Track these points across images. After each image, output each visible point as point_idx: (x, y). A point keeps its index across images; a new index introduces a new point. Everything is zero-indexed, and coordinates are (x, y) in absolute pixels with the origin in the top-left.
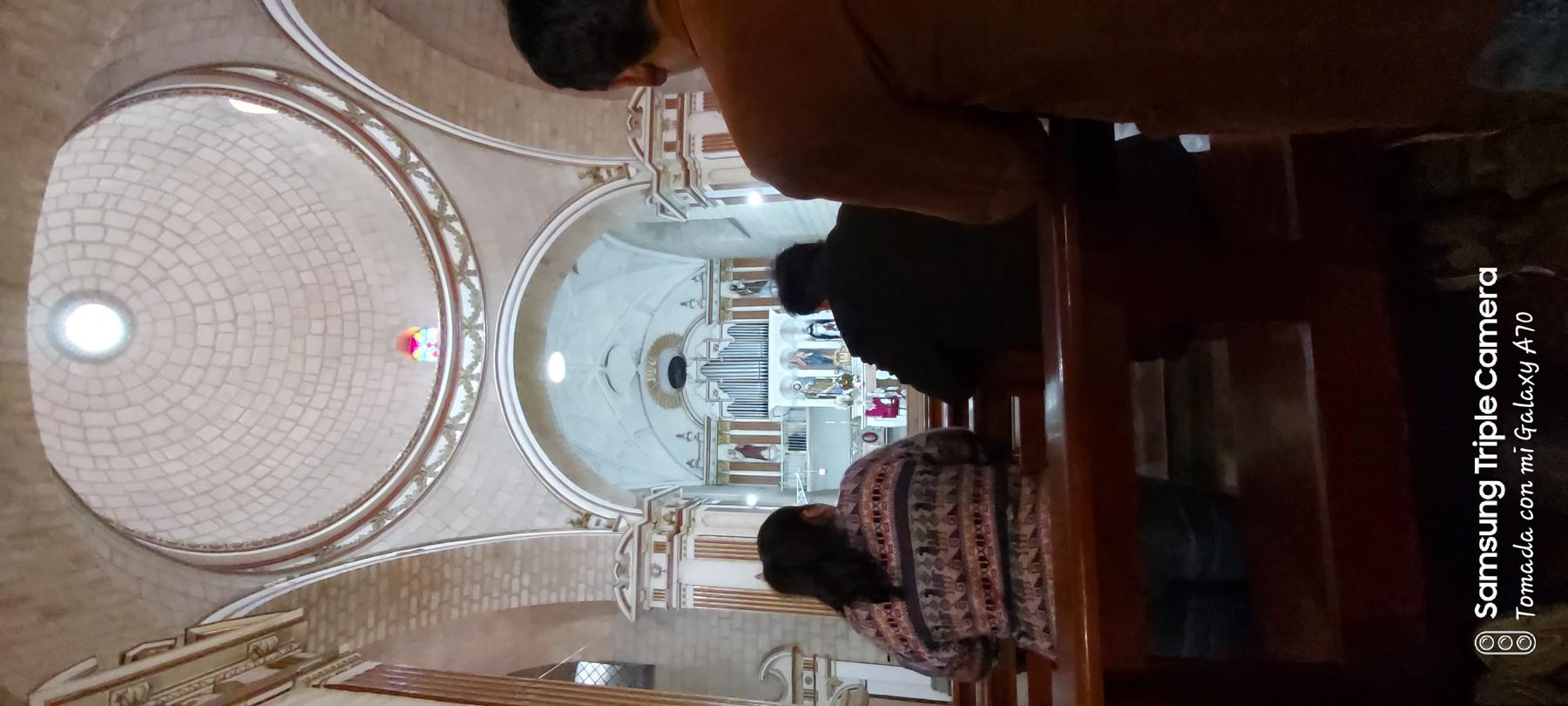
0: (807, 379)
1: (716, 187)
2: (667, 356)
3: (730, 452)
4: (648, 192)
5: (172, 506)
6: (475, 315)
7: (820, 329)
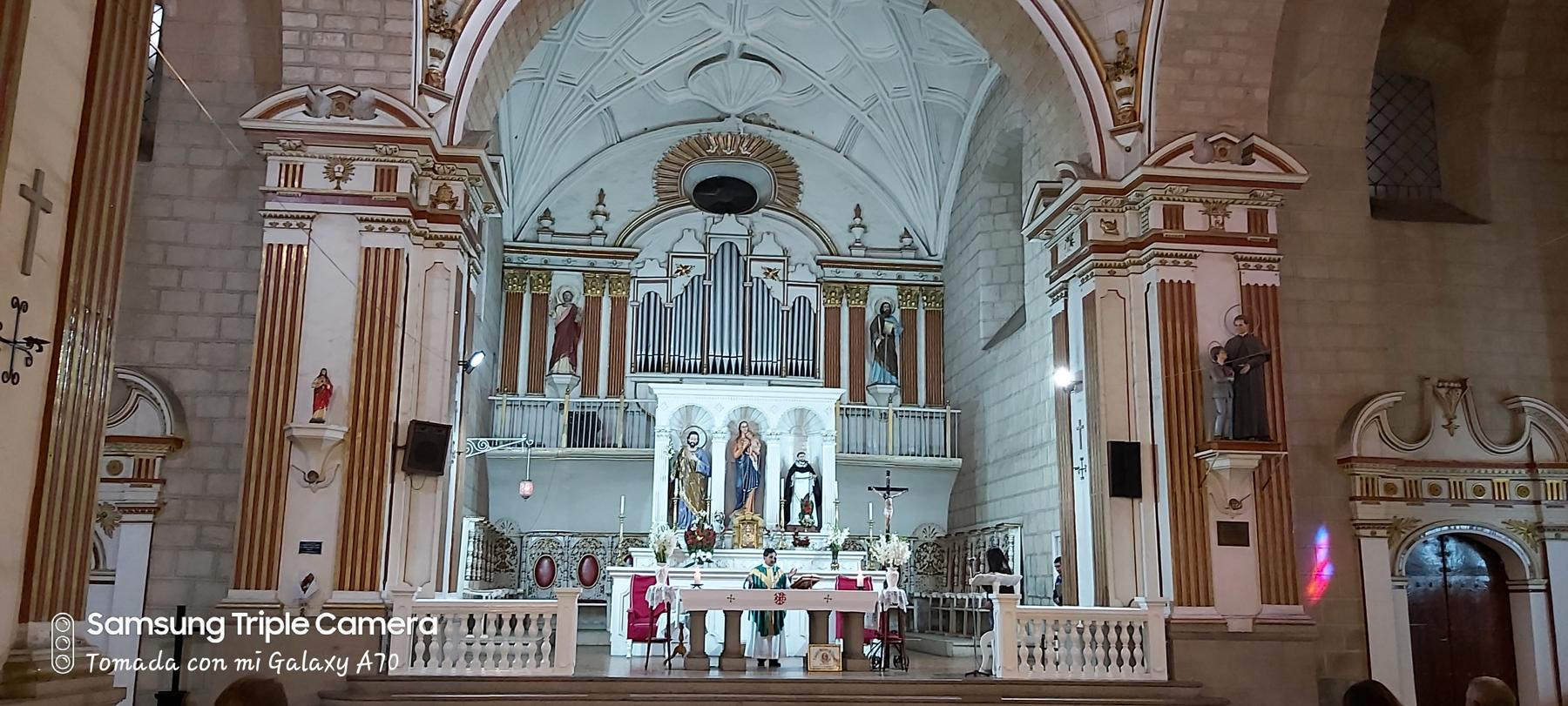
1: (1089, 302)
2: (757, 176)
3: (568, 297)
4: (1085, 168)
7: (803, 486)
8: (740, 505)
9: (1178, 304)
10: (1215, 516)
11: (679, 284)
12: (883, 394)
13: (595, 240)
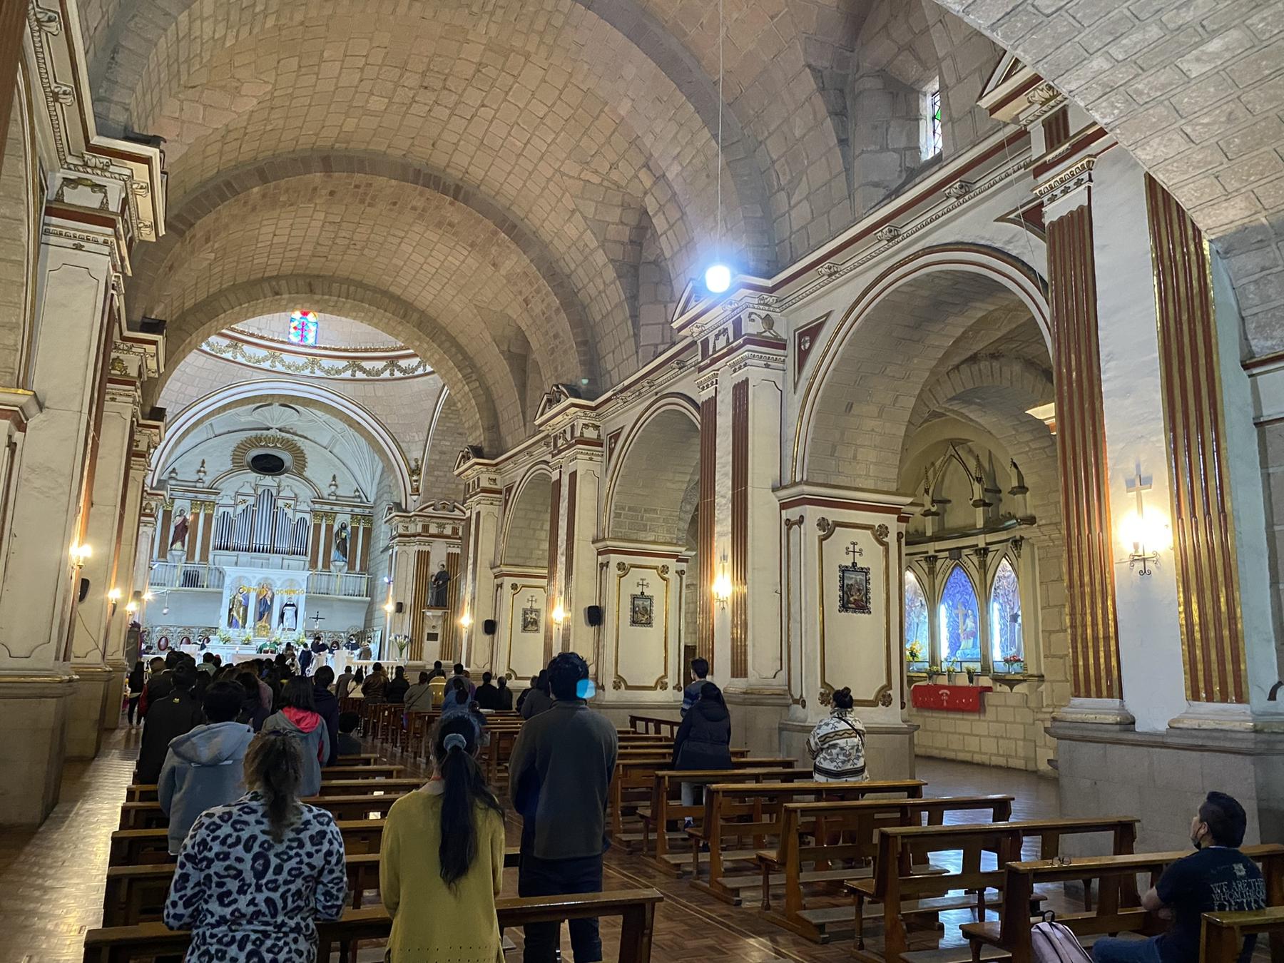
0: (247, 599)
5: (181, 35)
6: (322, 369)
8: (260, 619)
9: (423, 558)
10: (427, 631)
11: (240, 508)
12: (339, 564)
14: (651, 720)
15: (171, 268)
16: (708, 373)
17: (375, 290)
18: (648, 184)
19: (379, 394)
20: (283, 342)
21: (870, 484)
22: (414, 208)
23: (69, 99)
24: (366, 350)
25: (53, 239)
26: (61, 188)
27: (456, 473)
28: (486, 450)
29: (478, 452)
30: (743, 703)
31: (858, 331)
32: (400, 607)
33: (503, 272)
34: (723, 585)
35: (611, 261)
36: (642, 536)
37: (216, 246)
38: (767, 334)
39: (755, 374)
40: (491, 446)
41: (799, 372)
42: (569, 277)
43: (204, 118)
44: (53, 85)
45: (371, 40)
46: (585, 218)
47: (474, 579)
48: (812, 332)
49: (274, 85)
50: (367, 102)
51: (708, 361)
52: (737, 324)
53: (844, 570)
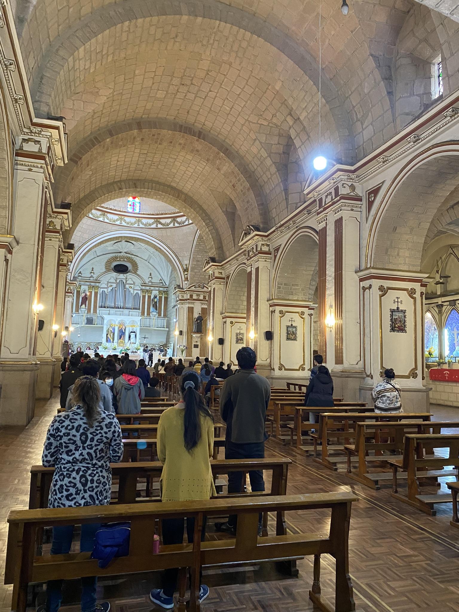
0: (114, 329)
4: (179, 286)
6: (143, 224)
8: (120, 338)
9: (191, 310)
10: (194, 343)
12: (154, 313)
13: (91, 279)
14: (297, 385)
15: (73, 179)
16: (322, 215)
17: (164, 185)
18: (291, 123)
19: (169, 234)
20: (125, 212)
21: (406, 268)
22: (180, 144)
23: (22, 102)
24: (162, 214)
25: (19, 167)
26: (22, 143)
27: (204, 270)
28: (217, 259)
29: (213, 260)
30: (340, 377)
31: (398, 190)
32: (181, 333)
33: (222, 172)
34: (330, 320)
35: (274, 163)
36: (291, 297)
37: (92, 168)
38: (352, 194)
39: (346, 214)
40: (219, 257)
41: (369, 212)
42: (254, 172)
43: (83, 108)
44: (15, 95)
45: (157, 63)
46: (261, 143)
47: (213, 319)
48: (375, 192)
49: (114, 89)
50: (156, 94)
51: (322, 209)
52: (337, 190)
53: (392, 311)
